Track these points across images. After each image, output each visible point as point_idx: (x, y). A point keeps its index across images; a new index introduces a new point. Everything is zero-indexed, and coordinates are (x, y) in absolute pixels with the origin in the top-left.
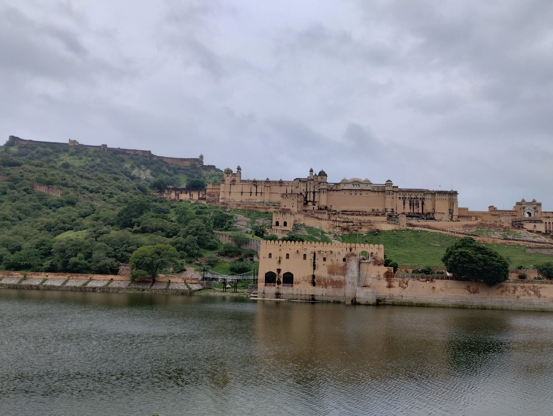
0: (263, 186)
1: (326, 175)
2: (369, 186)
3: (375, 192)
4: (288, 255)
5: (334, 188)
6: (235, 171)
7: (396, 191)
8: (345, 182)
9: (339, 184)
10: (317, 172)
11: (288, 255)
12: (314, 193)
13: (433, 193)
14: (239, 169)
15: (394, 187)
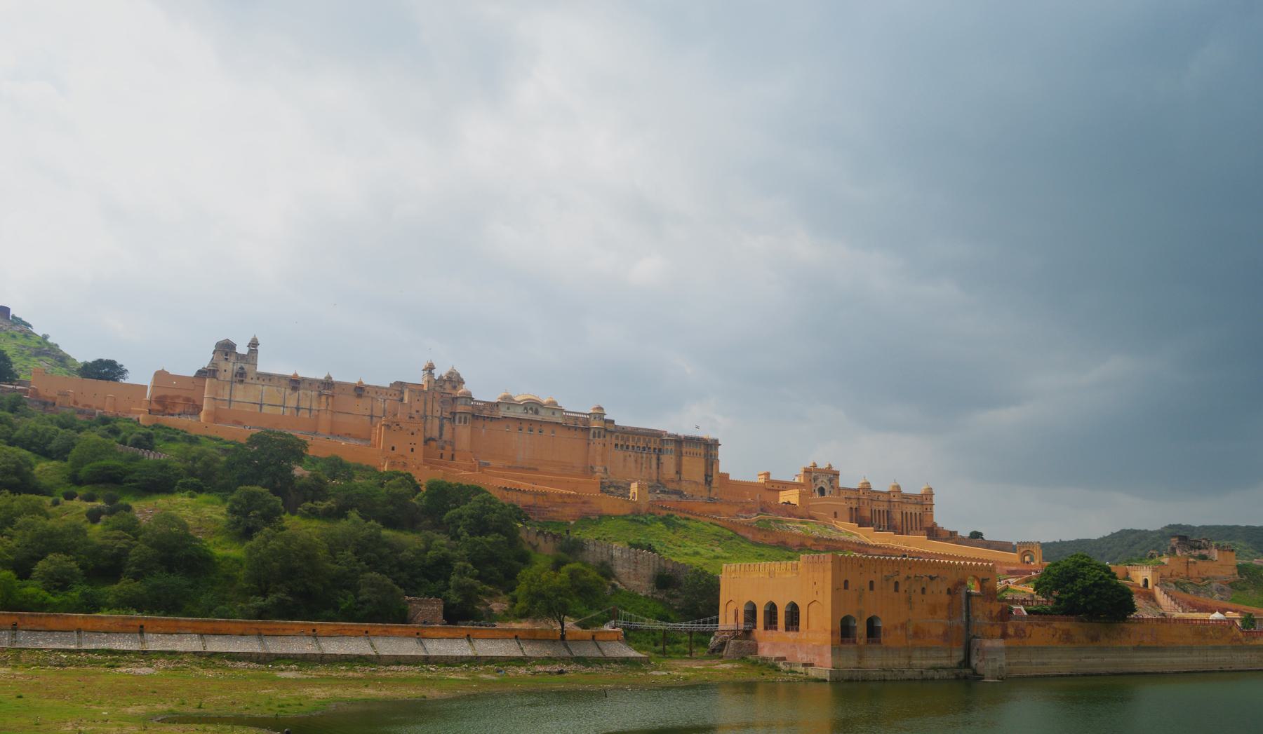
0: (315, 394)
1: (461, 382)
2: (557, 415)
3: (569, 428)
4: (871, 583)
5: (483, 415)
6: (242, 349)
7: (609, 429)
8: (508, 402)
9: (497, 404)
10: (441, 371)
11: (871, 583)
12: (442, 419)
13: (679, 441)
14: (254, 344)
15: (606, 421)
